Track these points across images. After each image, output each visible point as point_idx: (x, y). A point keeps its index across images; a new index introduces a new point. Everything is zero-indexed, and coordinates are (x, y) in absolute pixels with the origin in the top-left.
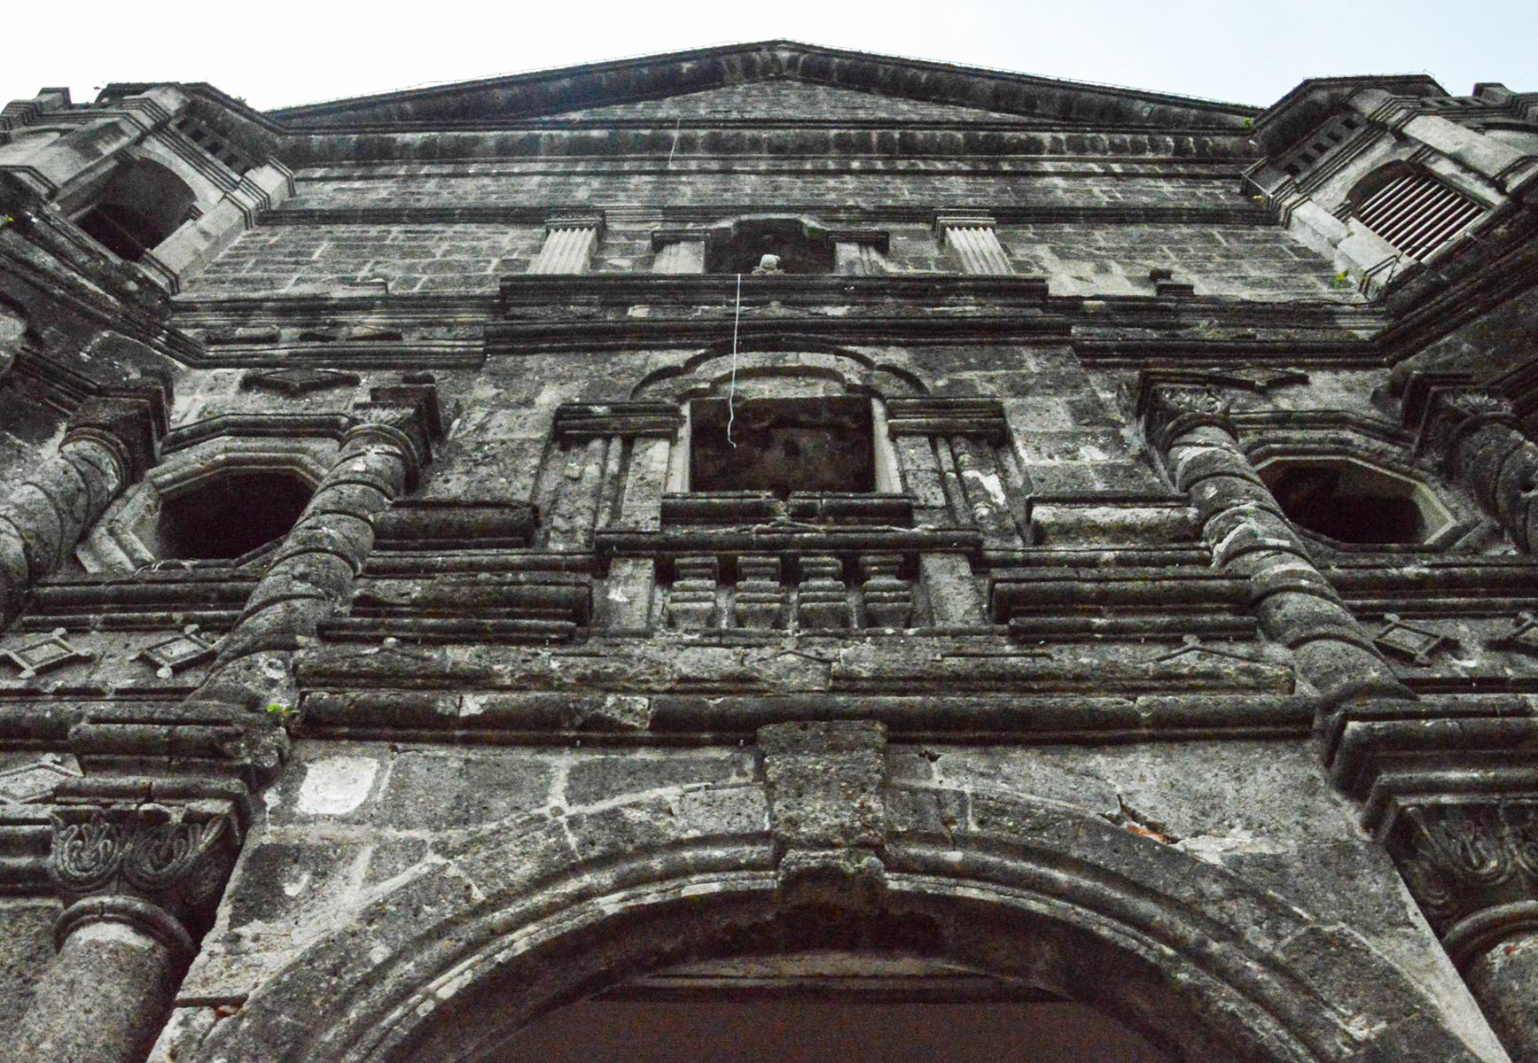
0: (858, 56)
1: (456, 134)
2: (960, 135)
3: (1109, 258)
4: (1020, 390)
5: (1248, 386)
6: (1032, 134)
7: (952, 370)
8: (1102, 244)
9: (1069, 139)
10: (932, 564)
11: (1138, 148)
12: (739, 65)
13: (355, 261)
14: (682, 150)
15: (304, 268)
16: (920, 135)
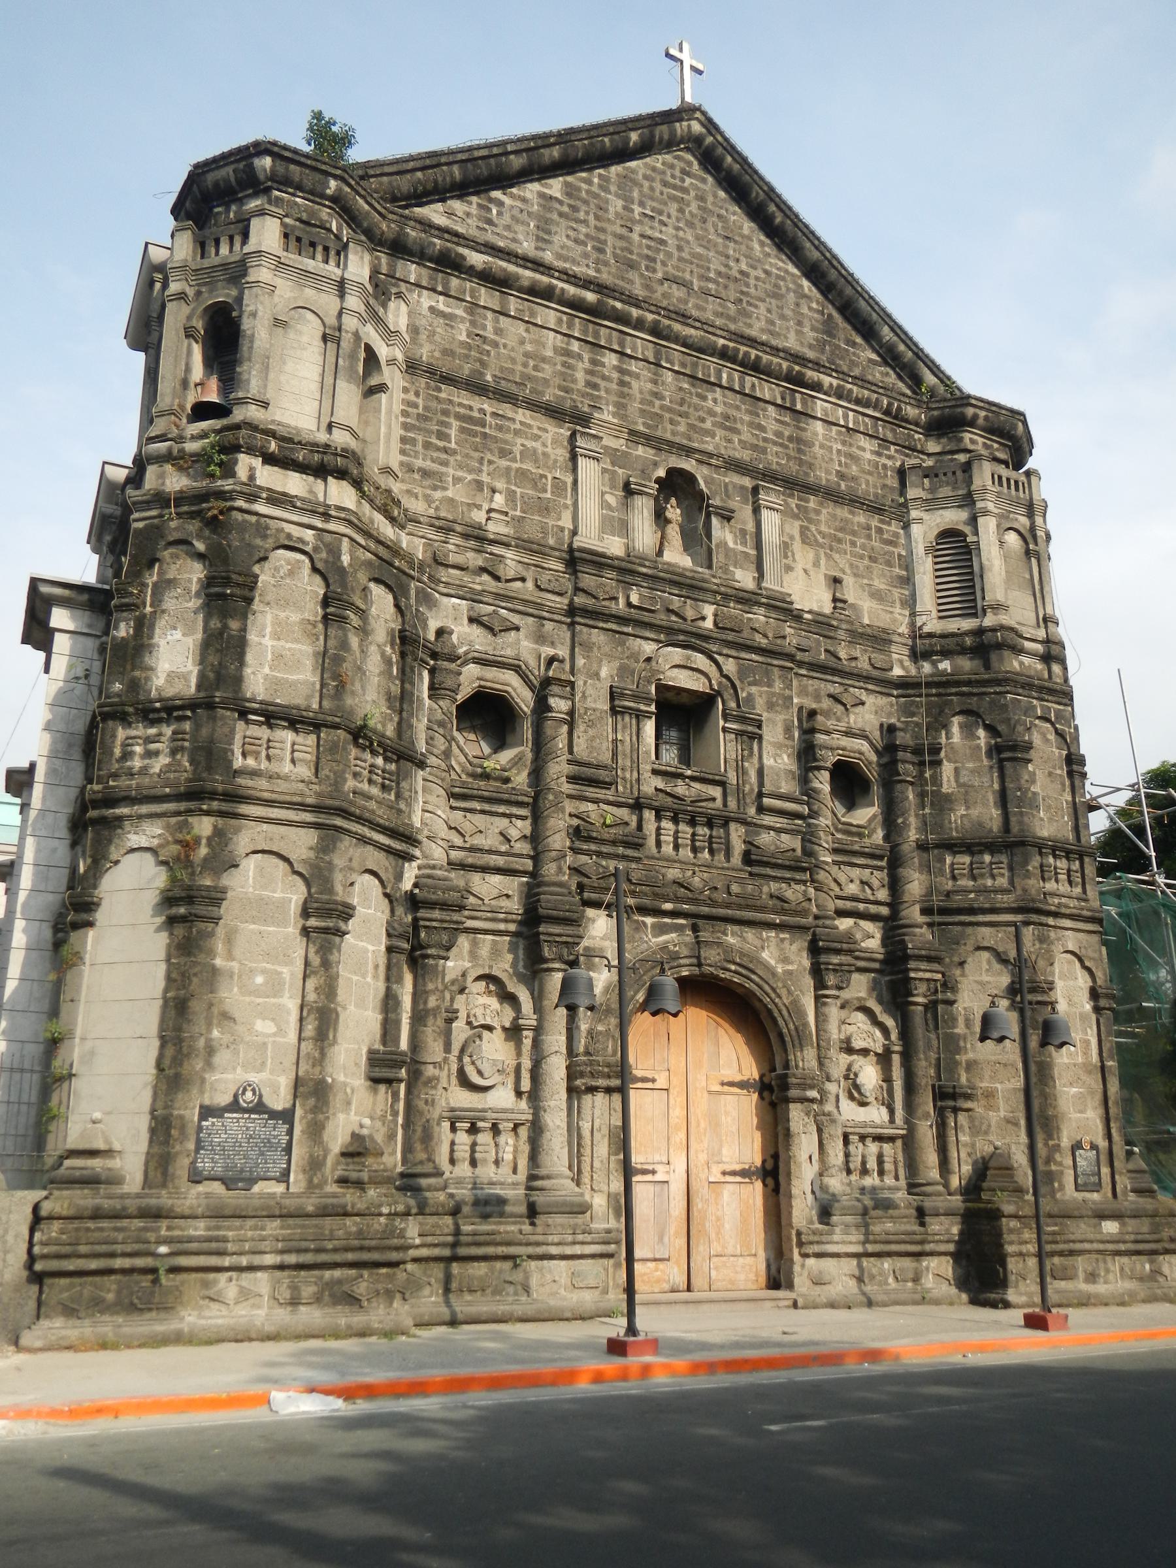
0: (743, 161)
1: (504, 264)
2: (785, 365)
3: (822, 546)
4: (770, 706)
5: (844, 705)
6: (822, 376)
7: (750, 684)
8: (823, 528)
9: (839, 386)
10: (733, 826)
11: (867, 404)
12: (666, 137)
13: (476, 455)
14: (635, 328)
15: (451, 459)
16: (765, 358)
